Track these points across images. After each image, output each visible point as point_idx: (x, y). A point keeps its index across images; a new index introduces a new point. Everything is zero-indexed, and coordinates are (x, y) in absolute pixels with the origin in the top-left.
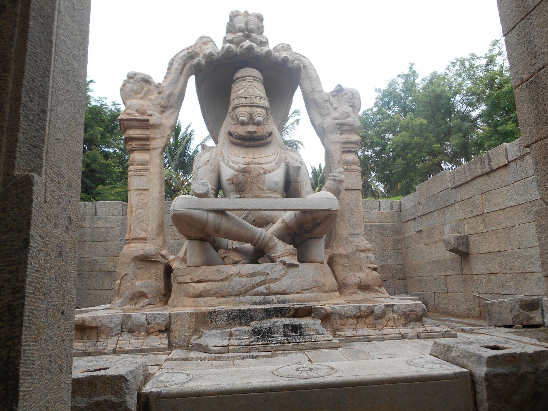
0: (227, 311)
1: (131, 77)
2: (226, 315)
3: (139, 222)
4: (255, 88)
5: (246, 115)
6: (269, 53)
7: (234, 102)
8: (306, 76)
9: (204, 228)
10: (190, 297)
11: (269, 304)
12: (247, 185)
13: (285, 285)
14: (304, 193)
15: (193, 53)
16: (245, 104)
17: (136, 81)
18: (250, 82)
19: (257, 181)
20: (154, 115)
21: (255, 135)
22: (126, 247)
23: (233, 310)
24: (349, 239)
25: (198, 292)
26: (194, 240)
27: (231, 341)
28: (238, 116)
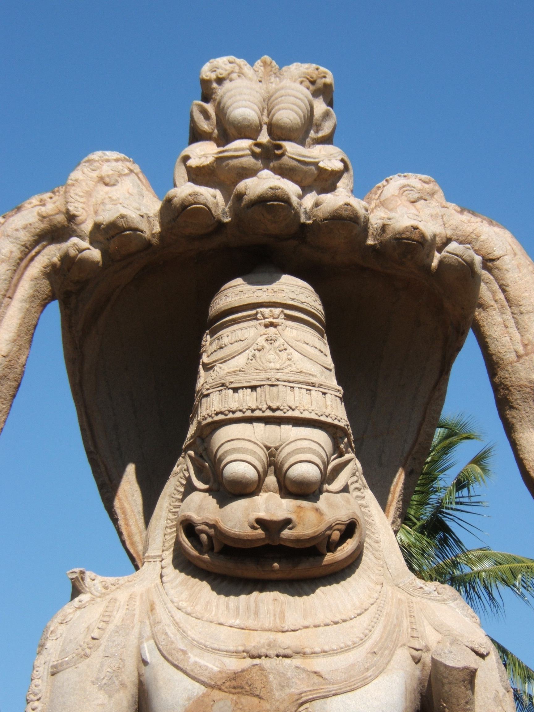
4: (290, 350)
5: (254, 453)
15: (61, 218)
16: (249, 414)
18: (272, 325)
28: (220, 461)
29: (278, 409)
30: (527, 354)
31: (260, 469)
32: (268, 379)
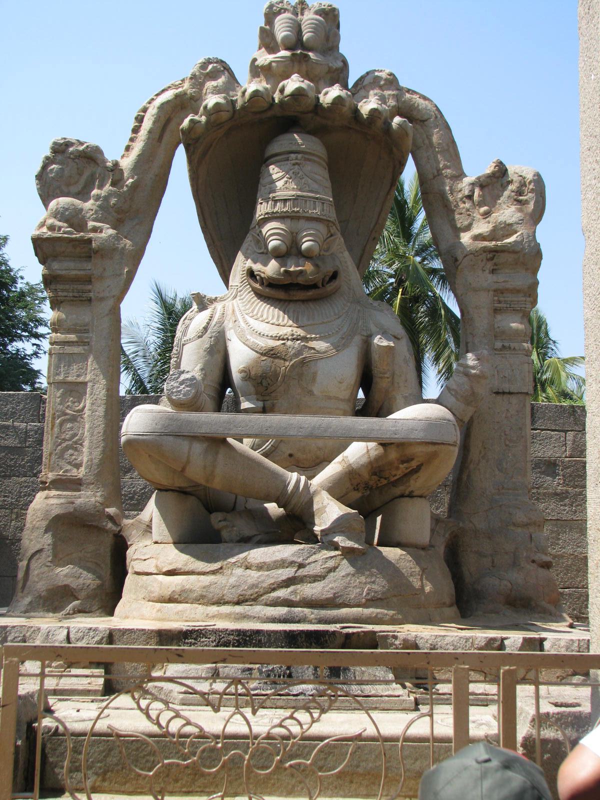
0: (215, 632)
1: (60, 149)
2: (213, 638)
3: (67, 448)
6: (338, 100)
7: (262, 209)
8: (427, 142)
9: (183, 470)
10: (153, 601)
11: (299, 622)
12: (279, 384)
13: (332, 588)
14: (399, 400)
16: (283, 214)
17: (69, 158)
18: (297, 164)
19: (301, 376)
20: (101, 232)
21: (300, 280)
22: (40, 496)
23: (227, 630)
24: (497, 497)
25: (167, 593)
26: (167, 490)
27: (214, 686)
28: (267, 240)
29: (298, 212)
30: (438, 175)
31: (288, 245)
32: (293, 196)
